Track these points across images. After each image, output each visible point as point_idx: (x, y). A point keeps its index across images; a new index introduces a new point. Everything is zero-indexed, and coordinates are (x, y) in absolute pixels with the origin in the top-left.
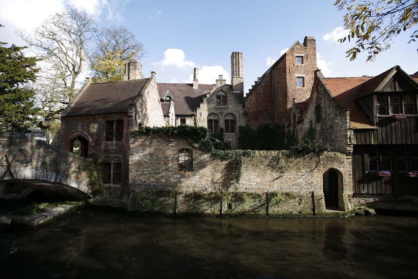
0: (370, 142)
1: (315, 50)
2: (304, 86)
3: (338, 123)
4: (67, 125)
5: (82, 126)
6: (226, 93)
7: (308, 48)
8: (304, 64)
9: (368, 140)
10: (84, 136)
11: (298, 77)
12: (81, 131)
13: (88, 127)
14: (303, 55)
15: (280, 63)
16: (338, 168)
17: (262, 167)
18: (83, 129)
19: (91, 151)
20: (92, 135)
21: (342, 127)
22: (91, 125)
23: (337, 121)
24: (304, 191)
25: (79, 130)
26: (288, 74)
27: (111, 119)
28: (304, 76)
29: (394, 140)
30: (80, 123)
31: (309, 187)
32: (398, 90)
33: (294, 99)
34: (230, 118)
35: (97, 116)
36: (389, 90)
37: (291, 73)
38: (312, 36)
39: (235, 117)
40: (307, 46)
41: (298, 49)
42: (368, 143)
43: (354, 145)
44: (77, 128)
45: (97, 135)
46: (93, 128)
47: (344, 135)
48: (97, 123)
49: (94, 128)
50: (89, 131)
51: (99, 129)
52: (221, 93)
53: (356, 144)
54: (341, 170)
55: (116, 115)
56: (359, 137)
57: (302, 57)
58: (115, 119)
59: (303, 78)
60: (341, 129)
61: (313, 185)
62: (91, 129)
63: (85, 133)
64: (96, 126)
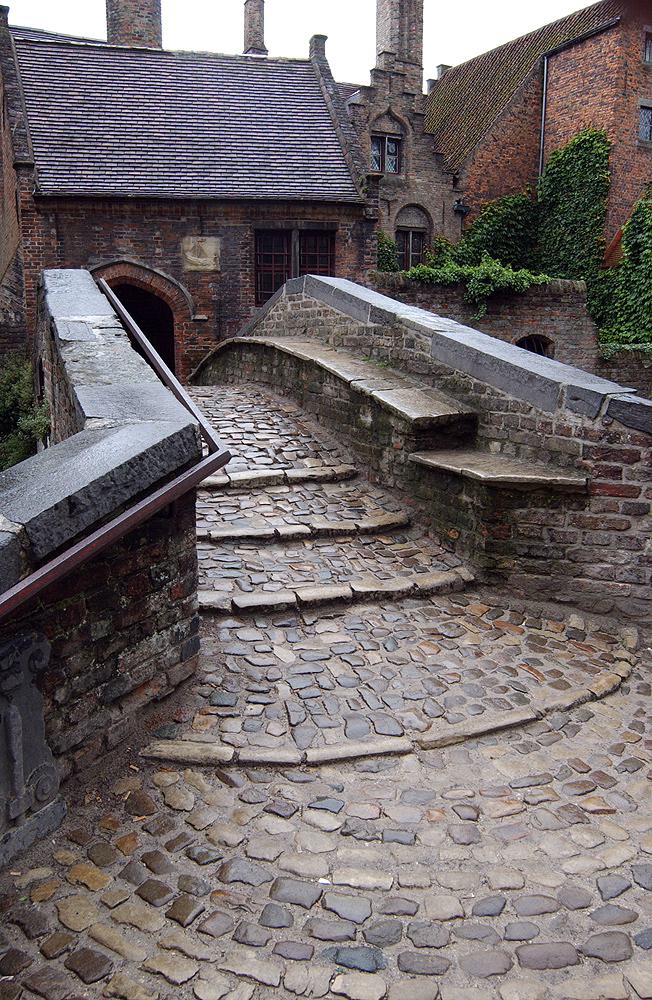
4: (59, 237)
5: (142, 245)
6: (403, 127)
10: (155, 283)
11: (642, 107)
12: (134, 261)
13: (176, 248)
15: (589, 43)
18: (150, 258)
19: (193, 341)
20: (195, 279)
22: (189, 243)
25: (125, 259)
27: (280, 224)
30: (128, 232)
34: (413, 221)
35: (221, 209)
39: (430, 221)
44: (113, 249)
45: (220, 283)
46: (200, 253)
48: (215, 234)
49: (204, 253)
50: (176, 267)
51: (224, 256)
52: (387, 126)
55: (309, 210)
58: (302, 224)
62: (190, 256)
63: (157, 270)
64: (212, 245)
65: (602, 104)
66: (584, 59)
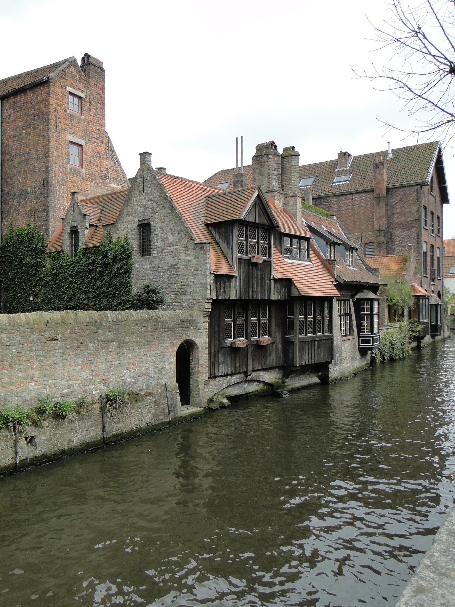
0: (230, 297)
1: (104, 93)
2: (82, 167)
3: (190, 261)
7: (92, 82)
8: (83, 117)
9: (227, 292)
11: (71, 142)
14: (82, 95)
16: (193, 339)
17: (91, 345)
21: (197, 270)
23: (188, 258)
24: (154, 383)
26: (52, 128)
28: (82, 142)
29: (251, 294)
31: (160, 376)
32: (257, 221)
33: (73, 193)
36: (249, 219)
37: (59, 128)
38: (100, 59)
40: (89, 77)
41: (73, 77)
42: (227, 298)
43: (213, 300)
47: (201, 284)
53: (215, 298)
54: (197, 341)
56: (218, 288)
57: (80, 98)
59: (81, 146)
60: (195, 272)
61: (165, 372)
65: (40, 136)
66: (27, 103)
